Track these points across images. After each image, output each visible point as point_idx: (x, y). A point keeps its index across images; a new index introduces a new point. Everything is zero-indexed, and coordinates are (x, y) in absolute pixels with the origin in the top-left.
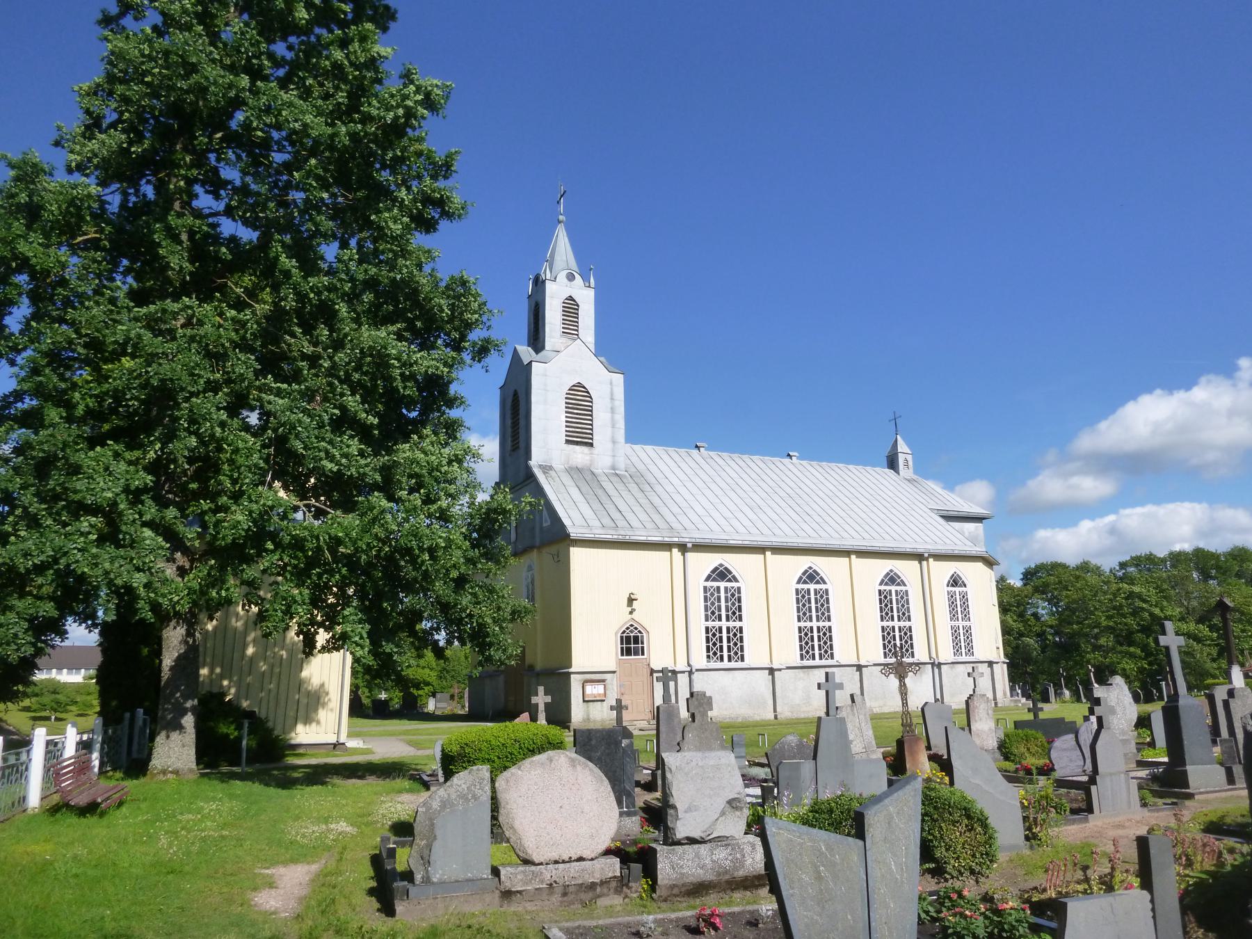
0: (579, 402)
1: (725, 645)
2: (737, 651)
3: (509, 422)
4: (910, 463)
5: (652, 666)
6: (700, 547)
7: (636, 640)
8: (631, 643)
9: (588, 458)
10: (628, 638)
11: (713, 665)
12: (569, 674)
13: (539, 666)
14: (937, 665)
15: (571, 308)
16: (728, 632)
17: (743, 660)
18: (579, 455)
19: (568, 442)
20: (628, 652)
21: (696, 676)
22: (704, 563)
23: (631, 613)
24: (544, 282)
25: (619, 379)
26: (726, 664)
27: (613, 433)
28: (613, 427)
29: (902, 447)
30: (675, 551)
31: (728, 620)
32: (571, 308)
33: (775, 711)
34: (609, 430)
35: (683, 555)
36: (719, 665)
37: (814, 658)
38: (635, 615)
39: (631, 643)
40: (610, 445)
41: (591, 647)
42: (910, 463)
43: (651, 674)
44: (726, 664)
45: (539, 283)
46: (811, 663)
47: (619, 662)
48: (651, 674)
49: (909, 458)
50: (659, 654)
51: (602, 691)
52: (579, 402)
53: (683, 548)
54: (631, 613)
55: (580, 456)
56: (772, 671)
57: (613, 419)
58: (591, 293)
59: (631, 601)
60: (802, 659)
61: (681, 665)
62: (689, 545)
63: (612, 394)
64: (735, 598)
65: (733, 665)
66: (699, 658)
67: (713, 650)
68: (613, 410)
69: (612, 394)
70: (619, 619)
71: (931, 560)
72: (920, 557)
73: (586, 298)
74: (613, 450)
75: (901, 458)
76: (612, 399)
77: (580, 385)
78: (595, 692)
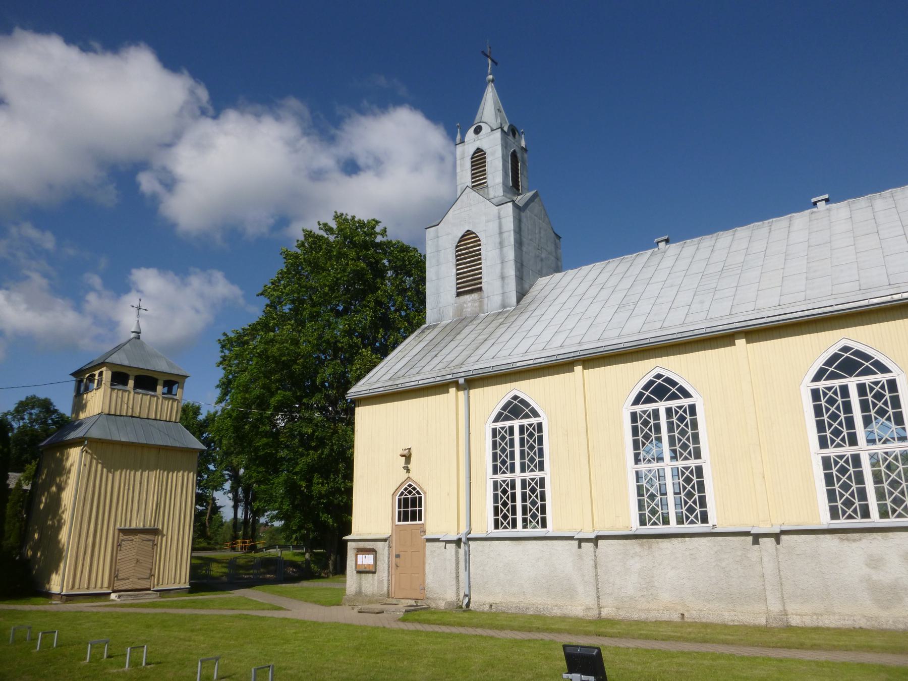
1: (520, 506)
2: (537, 513)
6: (473, 382)
8: (410, 506)
10: (406, 500)
11: (501, 533)
12: (347, 541)
16: (524, 486)
17: (544, 525)
20: (404, 517)
26: (519, 531)
27: (502, 268)
31: (523, 470)
37: (514, 526)
38: (411, 475)
39: (410, 506)
41: (371, 513)
46: (661, 529)
47: (395, 528)
50: (439, 519)
59: (408, 458)
60: (497, 526)
62: (461, 381)
64: (534, 438)
65: (530, 532)
66: (484, 523)
67: (503, 515)
68: (501, 244)
69: (500, 227)
70: (396, 478)
74: (503, 287)
76: (501, 233)
78: (365, 562)
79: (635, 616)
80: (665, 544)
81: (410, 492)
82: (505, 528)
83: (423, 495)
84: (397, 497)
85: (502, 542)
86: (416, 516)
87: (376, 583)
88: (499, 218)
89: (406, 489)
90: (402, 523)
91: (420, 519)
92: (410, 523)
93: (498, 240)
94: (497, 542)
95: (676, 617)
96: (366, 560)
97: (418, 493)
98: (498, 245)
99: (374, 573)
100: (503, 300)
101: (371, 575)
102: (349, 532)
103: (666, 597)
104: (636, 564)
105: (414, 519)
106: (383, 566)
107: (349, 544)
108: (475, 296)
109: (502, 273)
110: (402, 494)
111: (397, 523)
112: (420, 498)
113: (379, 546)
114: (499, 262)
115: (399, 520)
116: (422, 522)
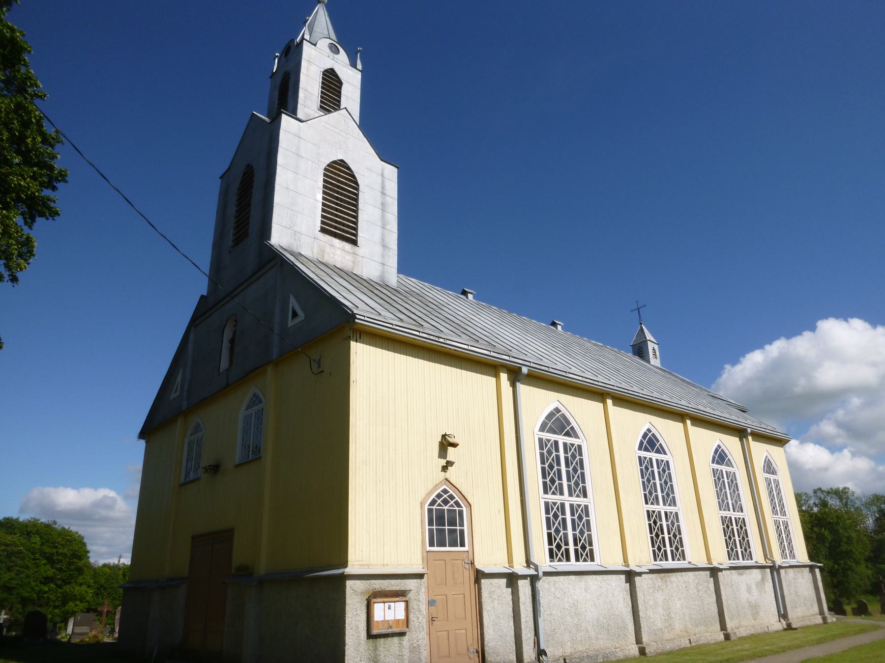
0: (340, 185)
3: (232, 209)
4: (658, 353)
5: (479, 566)
7: (455, 518)
8: (446, 522)
9: (349, 258)
12: (344, 578)
13: (262, 568)
14: (775, 569)
15: (331, 84)
17: (592, 560)
18: (336, 252)
19: (323, 230)
21: (541, 585)
22: (538, 402)
23: (445, 469)
24: (300, 44)
25: (391, 172)
27: (383, 234)
28: (383, 227)
29: (649, 336)
30: (504, 376)
32: (331, 84)
33: (639, 640)
34: (379, 231)
35: (513, 385)
36: (563, 566)
39: (446, 522)
40: (378, 249)
42: (658, 353)
43: (477, 581)
44: (573, 565)
45: (292, 54)
47: (427, 557)
48: (477, 581)
49: (656, 347)
51: (401, 616)
52: (340, 185)
53: (515, 375)
54: (445, 469)
55: (339, 252)
56: (630, 576)
57: (383, 217)
58: (358, 76)
61: (520, 567)
62: (525, 370)
63: (383, 187)
68: (383, 207)
69: (383, 187)
71: (750, 438)
72: (740, 433)
73: (352, 82)
74: (383, 256)
75: (650, 346)
76: (383, 193)
77: (342, 163)
78: (390, 616)
79: (668, 647)
80: (674, 577)
81: (446, 502)
82: (585, 560)
83: (464, 509)
84: (426, 507)
85: (609, 576)
86: (457, 539)
87: (406, 652)
88: (382, 175)
89: (439, 496)
90: (435, 549)
91: (463, 544)
92: (448, 549)
93: (379, 200)
94: (562, 578)
95: (685, 643)
96: (387, 613)
97: (457, 504)
98: (379, 206)
99: (402, 634)
100: (383, 272)
101: (396, 640)
102: (345, 565)
103: (678, 626)
104: (660, 597)
105: (453, 544)
106: (420, 619)
107: (349, 583)
108: (348, 246)
109: (383, 240)
110: (433, 503)
111: (429, 549)
112: (461, 513)
113: (411, 584)
114: (379, 223)
115: (431, 544)
116: (466, 549)
